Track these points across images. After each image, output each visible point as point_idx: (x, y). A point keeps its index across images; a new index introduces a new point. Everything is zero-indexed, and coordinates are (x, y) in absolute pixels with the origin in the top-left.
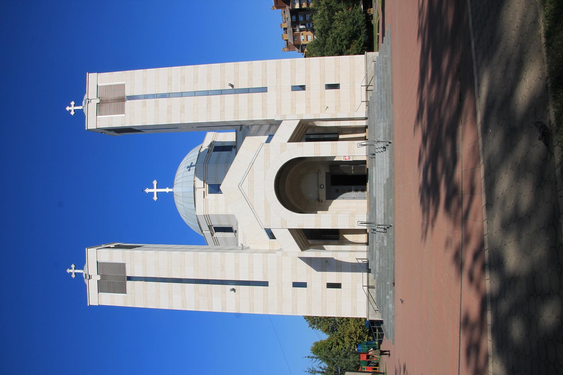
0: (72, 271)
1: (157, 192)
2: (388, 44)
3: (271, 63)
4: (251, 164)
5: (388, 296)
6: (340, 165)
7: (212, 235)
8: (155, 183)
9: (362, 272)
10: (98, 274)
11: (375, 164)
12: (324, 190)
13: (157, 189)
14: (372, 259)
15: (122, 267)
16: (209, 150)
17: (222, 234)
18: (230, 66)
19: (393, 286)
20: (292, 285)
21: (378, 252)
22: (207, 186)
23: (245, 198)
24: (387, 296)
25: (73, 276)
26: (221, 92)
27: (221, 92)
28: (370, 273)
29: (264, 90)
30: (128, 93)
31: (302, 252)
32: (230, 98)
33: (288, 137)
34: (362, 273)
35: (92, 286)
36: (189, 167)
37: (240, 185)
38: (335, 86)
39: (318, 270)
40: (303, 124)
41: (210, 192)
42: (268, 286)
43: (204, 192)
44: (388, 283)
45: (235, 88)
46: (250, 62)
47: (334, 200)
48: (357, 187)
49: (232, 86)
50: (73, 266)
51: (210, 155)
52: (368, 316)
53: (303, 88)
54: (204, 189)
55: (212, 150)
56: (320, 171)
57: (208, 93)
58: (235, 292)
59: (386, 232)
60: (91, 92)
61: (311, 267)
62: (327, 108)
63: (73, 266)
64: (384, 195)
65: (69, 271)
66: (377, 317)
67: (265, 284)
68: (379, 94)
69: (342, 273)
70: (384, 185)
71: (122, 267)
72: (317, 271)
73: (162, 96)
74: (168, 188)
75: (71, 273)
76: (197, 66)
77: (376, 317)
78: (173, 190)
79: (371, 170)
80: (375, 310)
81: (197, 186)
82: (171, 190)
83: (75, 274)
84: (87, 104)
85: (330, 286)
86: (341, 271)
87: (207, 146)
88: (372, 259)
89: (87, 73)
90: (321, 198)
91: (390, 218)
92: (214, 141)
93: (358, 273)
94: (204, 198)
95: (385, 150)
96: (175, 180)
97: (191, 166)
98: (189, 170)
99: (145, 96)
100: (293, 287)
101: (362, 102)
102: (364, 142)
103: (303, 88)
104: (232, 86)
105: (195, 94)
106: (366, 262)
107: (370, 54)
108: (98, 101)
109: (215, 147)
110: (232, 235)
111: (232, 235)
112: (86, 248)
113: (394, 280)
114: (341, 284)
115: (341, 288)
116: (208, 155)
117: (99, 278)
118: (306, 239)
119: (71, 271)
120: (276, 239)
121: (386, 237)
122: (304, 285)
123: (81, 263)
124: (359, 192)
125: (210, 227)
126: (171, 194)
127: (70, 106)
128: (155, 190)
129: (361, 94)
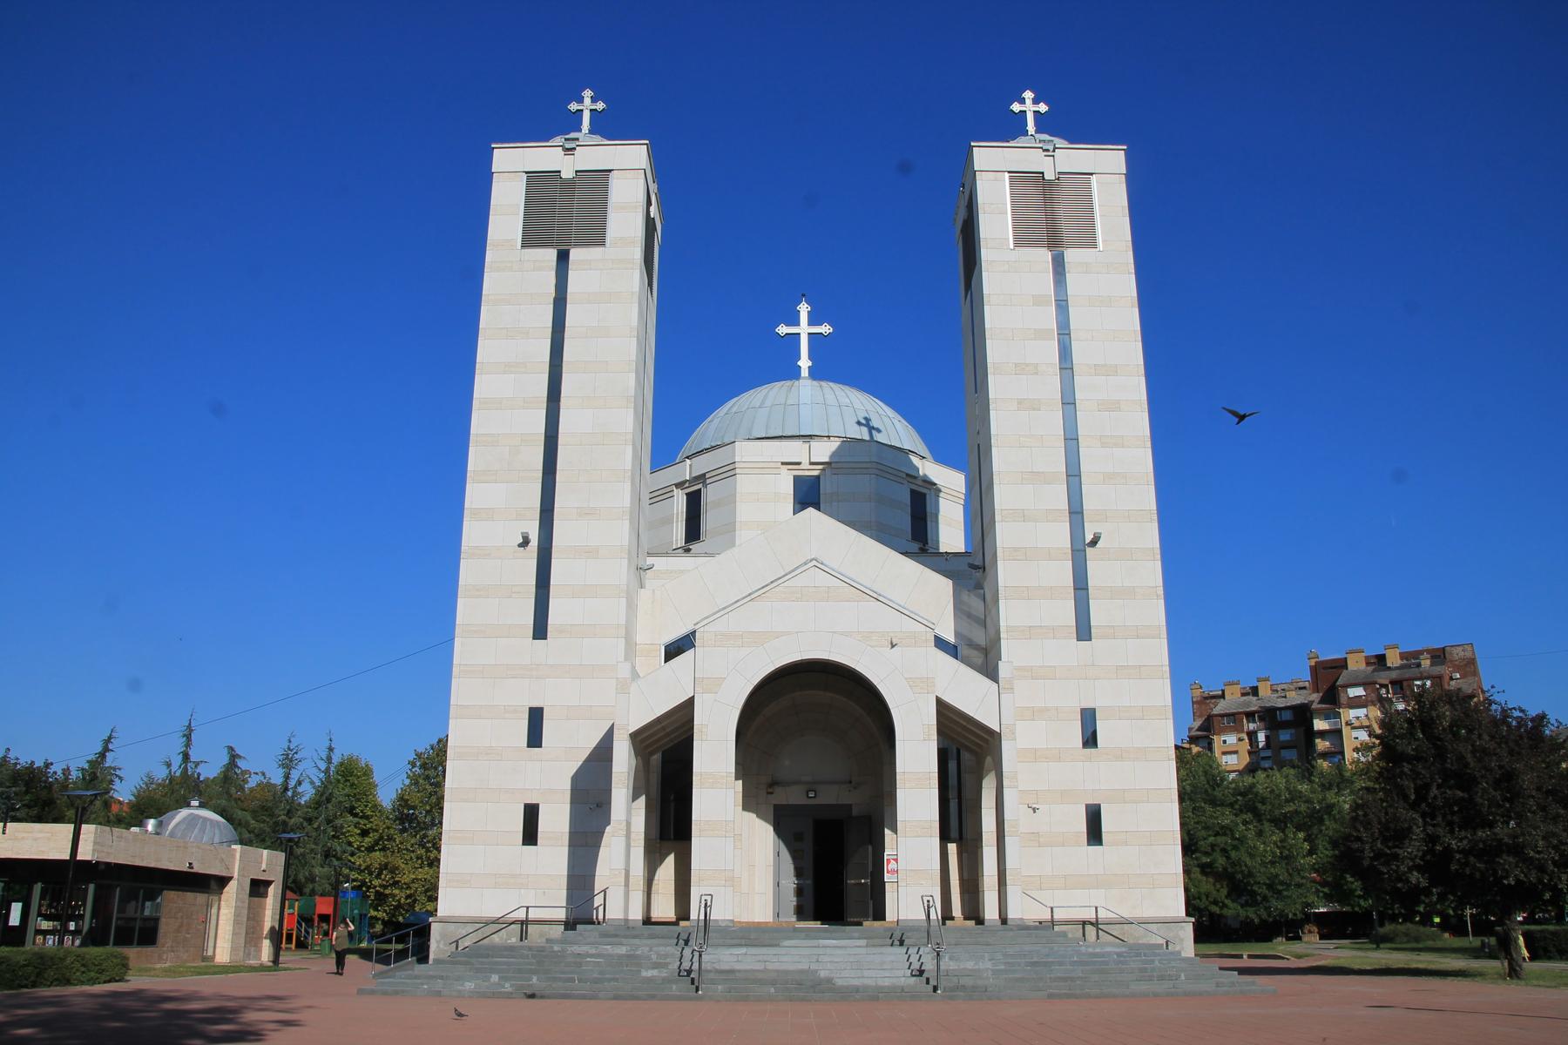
0: (588, 104)
1: (799, 334)
2: (1218, 985)
3: (1157, 652)
4: (875, 595)
6: (871, 844)
7: (679, 485)
8: (825, 329)
10: (576, 171)
11: (874, 946)
12: (802, 800)
13: (809, 334)
14: (605, 935)
15: (596, 237)
16: (915, 478)
17: (682, 512)
18: (1150, 536)
19: (525, 994)
20: (535, 704)
21: (624, 953)
22: (816, 473)
23: (780, 578)
24: (497, 977)
25: (574, 107)
26: (1076, 513)
27: (1076, 513)
28: (563, 927)
29: (1084, 631)
30: (1071, 255)
31: (627, 737)
32: (1060, 536)
33: (948, 699)
34: (565, 905)
35: (546, 157)
36: (867, 423)
37: (817, 564)
38: (1095, 833)
39: (576, 779)
40: (987, 741)
41: (798, 481)
42: (534, 639)
43: (799, 464)
44: (535, 979)
45: (1089, 550)
46: (1161, 591)
47: (772, 828)
48: (809, 893)
49: (1094, 543)
50: (600, 106)
51: (901, 481)
52: (443, 921)
53: (1090, 740)
54: (805, 465)
55: (914, 487)
56: (855, 788)
57: (1074, 475)
58: (520, 545)
60: (1072, 158)
62: (1034, 810)
63: (600, 106)
64: (786, 972)
65: (588, 94)
66: (438, 947)
67: (540, 631)
68: (1075, 959)
69: (567, 849)
70: (816, 971)
71: (596, 237)
73: (1064, 347)
74: (810, 364)
75: (581, 100)
76: (1149, 444)
77: (438, 942)
78: (805, 378)
79: (856, 935)
80: (457, 941)
81: (815, 444)
82: (805, 373)
83: (578, 110)
84: (1040, 145)
85: (531, 813)
87: (927, 473)
88: (605, 935)
89: (1125, 147)
90: (778, 790)
91: (720, 987)
92: (940, 491)
93: (564, 893)
94: (783, 463)
95: (915, 976)
96: (831, 384)
97: (871, 429)
98: (859, 423)
99: (1064, 303)
100: (530, 709)
101: (1052, 909)
102: (936, 914)
103: (1090, 740)
104: (1094, 543)
105: (1072, 440)
106: (595, 917)
107: (1188, 931)
108: (1049, 176)
109: (924, 495)
110: (677, 540)
111: (677, 540)
112: (647, 142)
113: (542, 997)
114: (536, 844)
116: (901, 474)
117: (567, 174)
118: (666, 748)
119: (587, 101)
120: (665, 662)
121: (665, 975)
122: (535, 739)
123: (609, 128)
124: (795, 899)
125: (702, 478)
126: (795, 374)
127: (1036, 101)
128: (804, 329)
129: (1073, 905)
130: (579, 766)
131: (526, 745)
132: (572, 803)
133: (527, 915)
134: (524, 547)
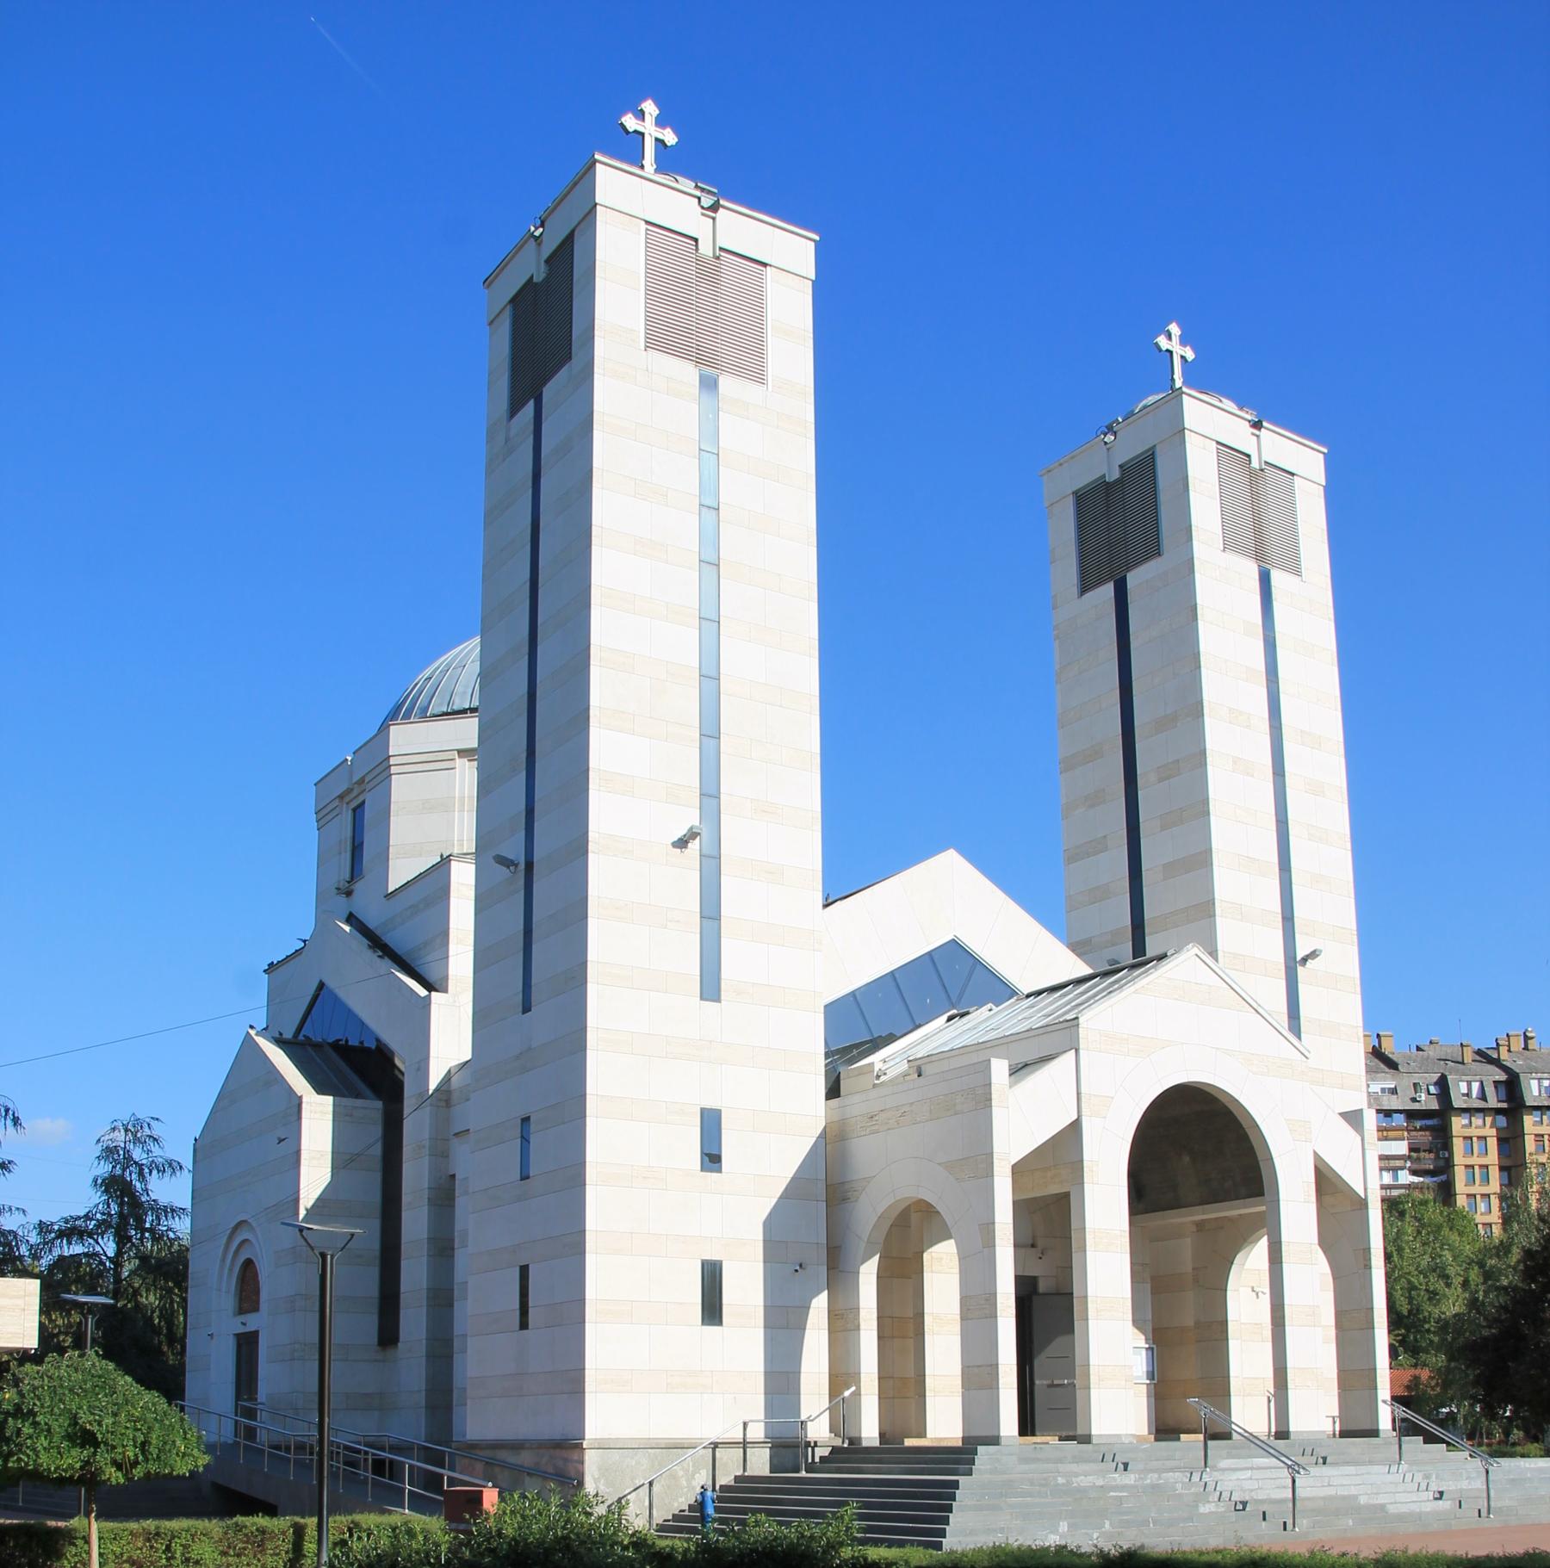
5: (1066, 1529)
9: (766, 1419)
21: (1132, 1482)
24: (1066, 1523)
28: (768, 1450)
34: (762, 1416)
39: (769, 1224)
52: (603, 1446)
53: (712, 1160)
59: (1236, 1510)
61: (778, 1195)
67: (711, 988)
69: (762, 1330)
70: (1355, 1497)
72: (765, 1223)
77: (596, 1481)
86: (769, 1325)
91: (1305, 1521)
93: (760, 1400)
103: (712, 1160)
114: (720, 1323)
115: (703, 1323)
130: (773, 1204)
131: (699, 1168)
132: (767, 1260)
133: (745, 1435)
134: (681, 848)
